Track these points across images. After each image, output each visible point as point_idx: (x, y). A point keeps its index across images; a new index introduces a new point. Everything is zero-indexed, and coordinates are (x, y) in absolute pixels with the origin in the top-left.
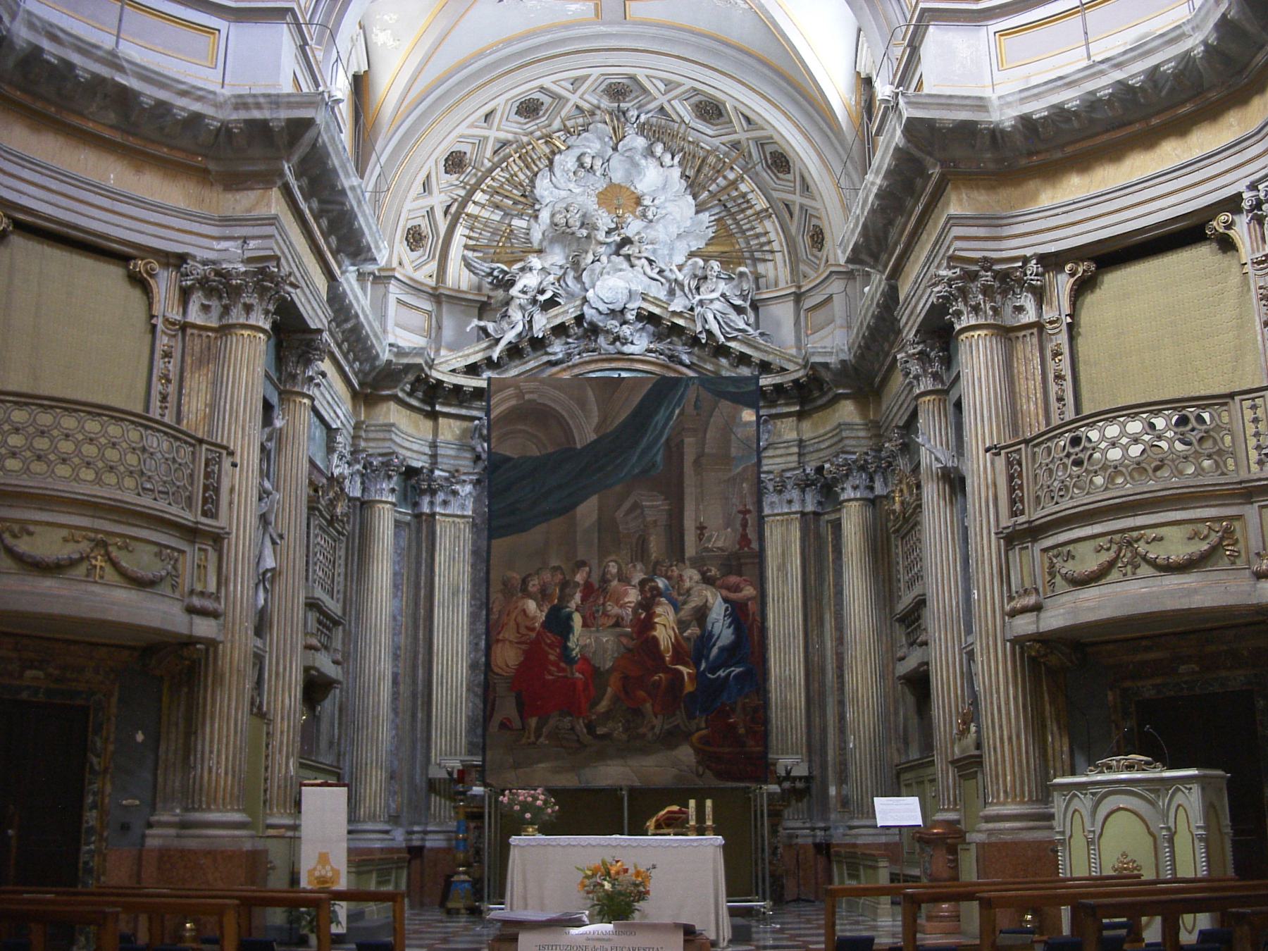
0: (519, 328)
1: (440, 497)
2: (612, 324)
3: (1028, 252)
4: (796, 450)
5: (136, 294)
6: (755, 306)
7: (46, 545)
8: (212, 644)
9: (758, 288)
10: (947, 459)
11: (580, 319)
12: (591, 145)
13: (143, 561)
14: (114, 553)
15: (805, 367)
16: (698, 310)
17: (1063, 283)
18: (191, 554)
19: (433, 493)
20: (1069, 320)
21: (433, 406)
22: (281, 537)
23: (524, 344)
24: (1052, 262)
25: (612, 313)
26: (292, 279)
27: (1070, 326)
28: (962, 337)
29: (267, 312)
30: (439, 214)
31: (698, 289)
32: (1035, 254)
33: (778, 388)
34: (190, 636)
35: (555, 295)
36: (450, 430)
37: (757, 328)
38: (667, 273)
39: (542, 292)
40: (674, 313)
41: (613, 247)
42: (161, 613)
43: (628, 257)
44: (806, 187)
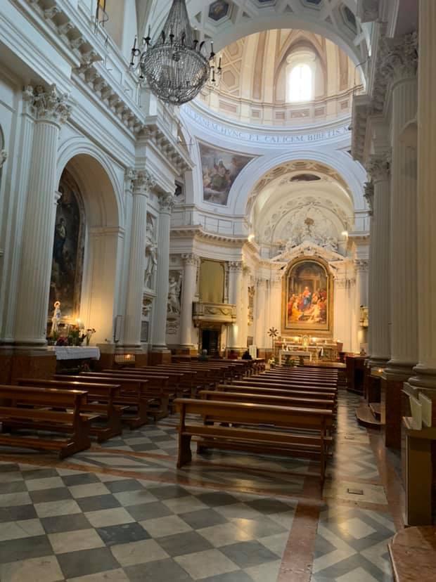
5: (222, 267)
6: (338, 245)
11: (300, 249)
42: (228, 319)
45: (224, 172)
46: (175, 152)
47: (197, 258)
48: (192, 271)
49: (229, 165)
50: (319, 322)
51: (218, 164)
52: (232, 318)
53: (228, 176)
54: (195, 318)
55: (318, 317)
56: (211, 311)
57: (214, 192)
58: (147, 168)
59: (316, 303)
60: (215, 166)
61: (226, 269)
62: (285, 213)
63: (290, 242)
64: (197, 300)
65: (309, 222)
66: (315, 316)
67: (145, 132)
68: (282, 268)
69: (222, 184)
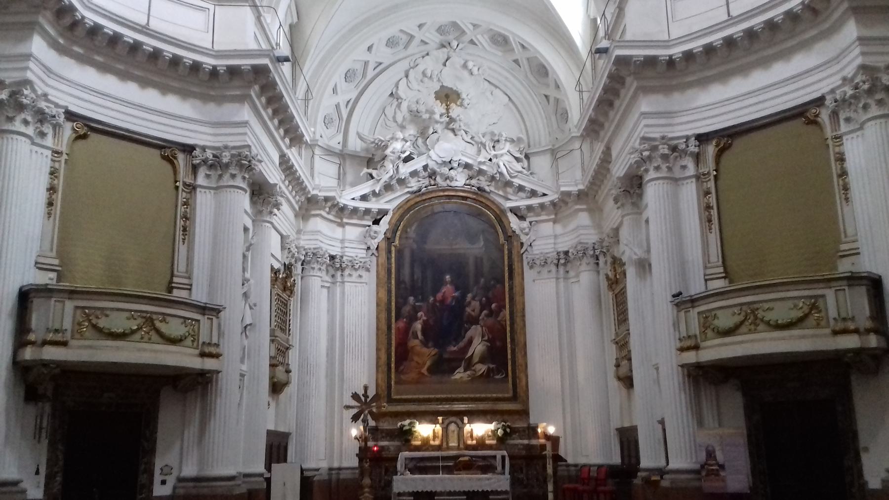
0: (391, 173)
1: (347, 272)
2: (445, 170)
3: (689, 133)
4: (552, 241)
6: (527, 157)
7: (118, 322)
9: (529, 146)
10: (640, 253)
11: (425, 167)
12: (429, 65)
13: (174, 328)
14: (158, 324)
15: (557, 193)
16: (494, 160)
17: (711, 150)
18: (204, 320)
19: (343, 270)
20: (715, 173)
21: (342, 219)
22: (255, 305)
23: (394, 182)
24: (702, 139)
25: (444, 163)
26: (259, 157)
27: (715, 177)
28: (649, 184)
29: (244, 178)
30: (343, 107)
31: (494, 147)
32: (694, 134)
33: (542, 206)
34: (202, 370)
35: (411, 153)
36: (353, 232)
37: (529, 169)
38: (476, 139)
39: (404, 152)
40: (480, 163)
41: (444, 125)
42: (184, 358)
43: (453, 130)
44: (558, 87)
47: (51, 110)
50: (487, 376)
52: (203, 355)
54: (28, 354)
55: (482, 361)
56: (102, 323)
59: (475, 321)
61: (184, 175)
62: (381, 69)
63: (398, 146)
65: (448, 96)
66: (476, 359)
68: (376, 222)
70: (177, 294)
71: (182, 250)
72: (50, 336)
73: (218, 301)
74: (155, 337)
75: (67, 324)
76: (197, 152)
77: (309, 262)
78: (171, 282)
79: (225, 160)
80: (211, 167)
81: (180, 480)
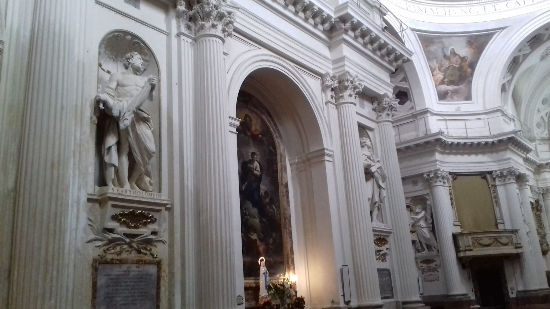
5: (484, 180)
7: (486, 241)
8: (522, 253)
13: (504, 240)
18: (513, 235)
30: (544, 117)
45: (459, 61)
46: (382, 42)
47: (444, 174)
48: (443, 194)
49: (464, 51)
51: (448, 53)
52: (516, 248)
53: (466, 65)
54: (462, 254)
56: (481, 242)
57: (451, 88)
58: (347, 69)
60: (445, 56)
61: (491, 182)
64: (458, 230)
67: (337, 27)
69: (460, 76)
70: (501, 227)
71: (497, 210)
72: (467, 248)
73: (516, 228)
74: (499, 244)
75: (471, 244)
76: (494, 173)
77: (545, 194)
78: (496, 222)
79: (505, 174)
80: (500, 177)
81: (518, 292)
